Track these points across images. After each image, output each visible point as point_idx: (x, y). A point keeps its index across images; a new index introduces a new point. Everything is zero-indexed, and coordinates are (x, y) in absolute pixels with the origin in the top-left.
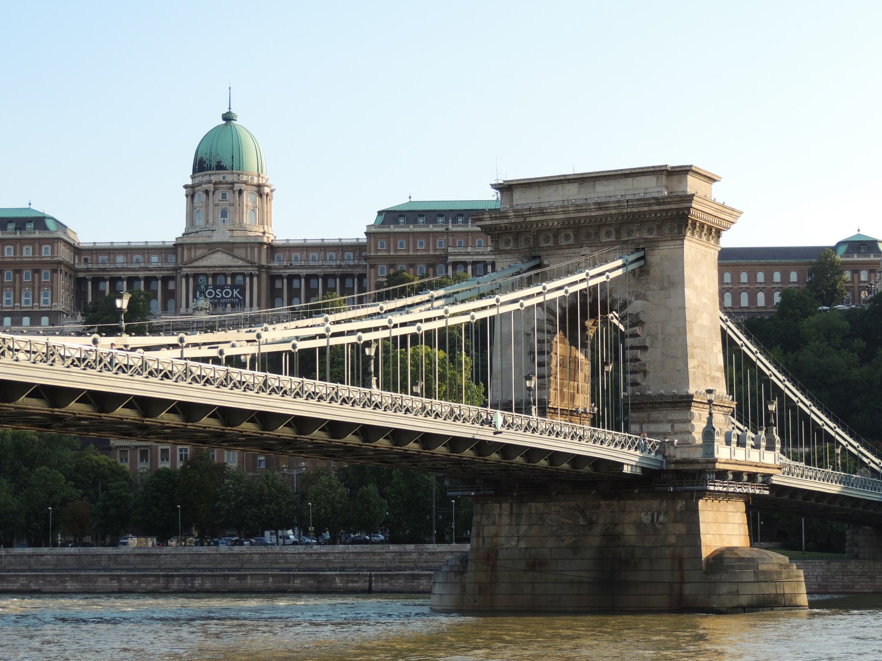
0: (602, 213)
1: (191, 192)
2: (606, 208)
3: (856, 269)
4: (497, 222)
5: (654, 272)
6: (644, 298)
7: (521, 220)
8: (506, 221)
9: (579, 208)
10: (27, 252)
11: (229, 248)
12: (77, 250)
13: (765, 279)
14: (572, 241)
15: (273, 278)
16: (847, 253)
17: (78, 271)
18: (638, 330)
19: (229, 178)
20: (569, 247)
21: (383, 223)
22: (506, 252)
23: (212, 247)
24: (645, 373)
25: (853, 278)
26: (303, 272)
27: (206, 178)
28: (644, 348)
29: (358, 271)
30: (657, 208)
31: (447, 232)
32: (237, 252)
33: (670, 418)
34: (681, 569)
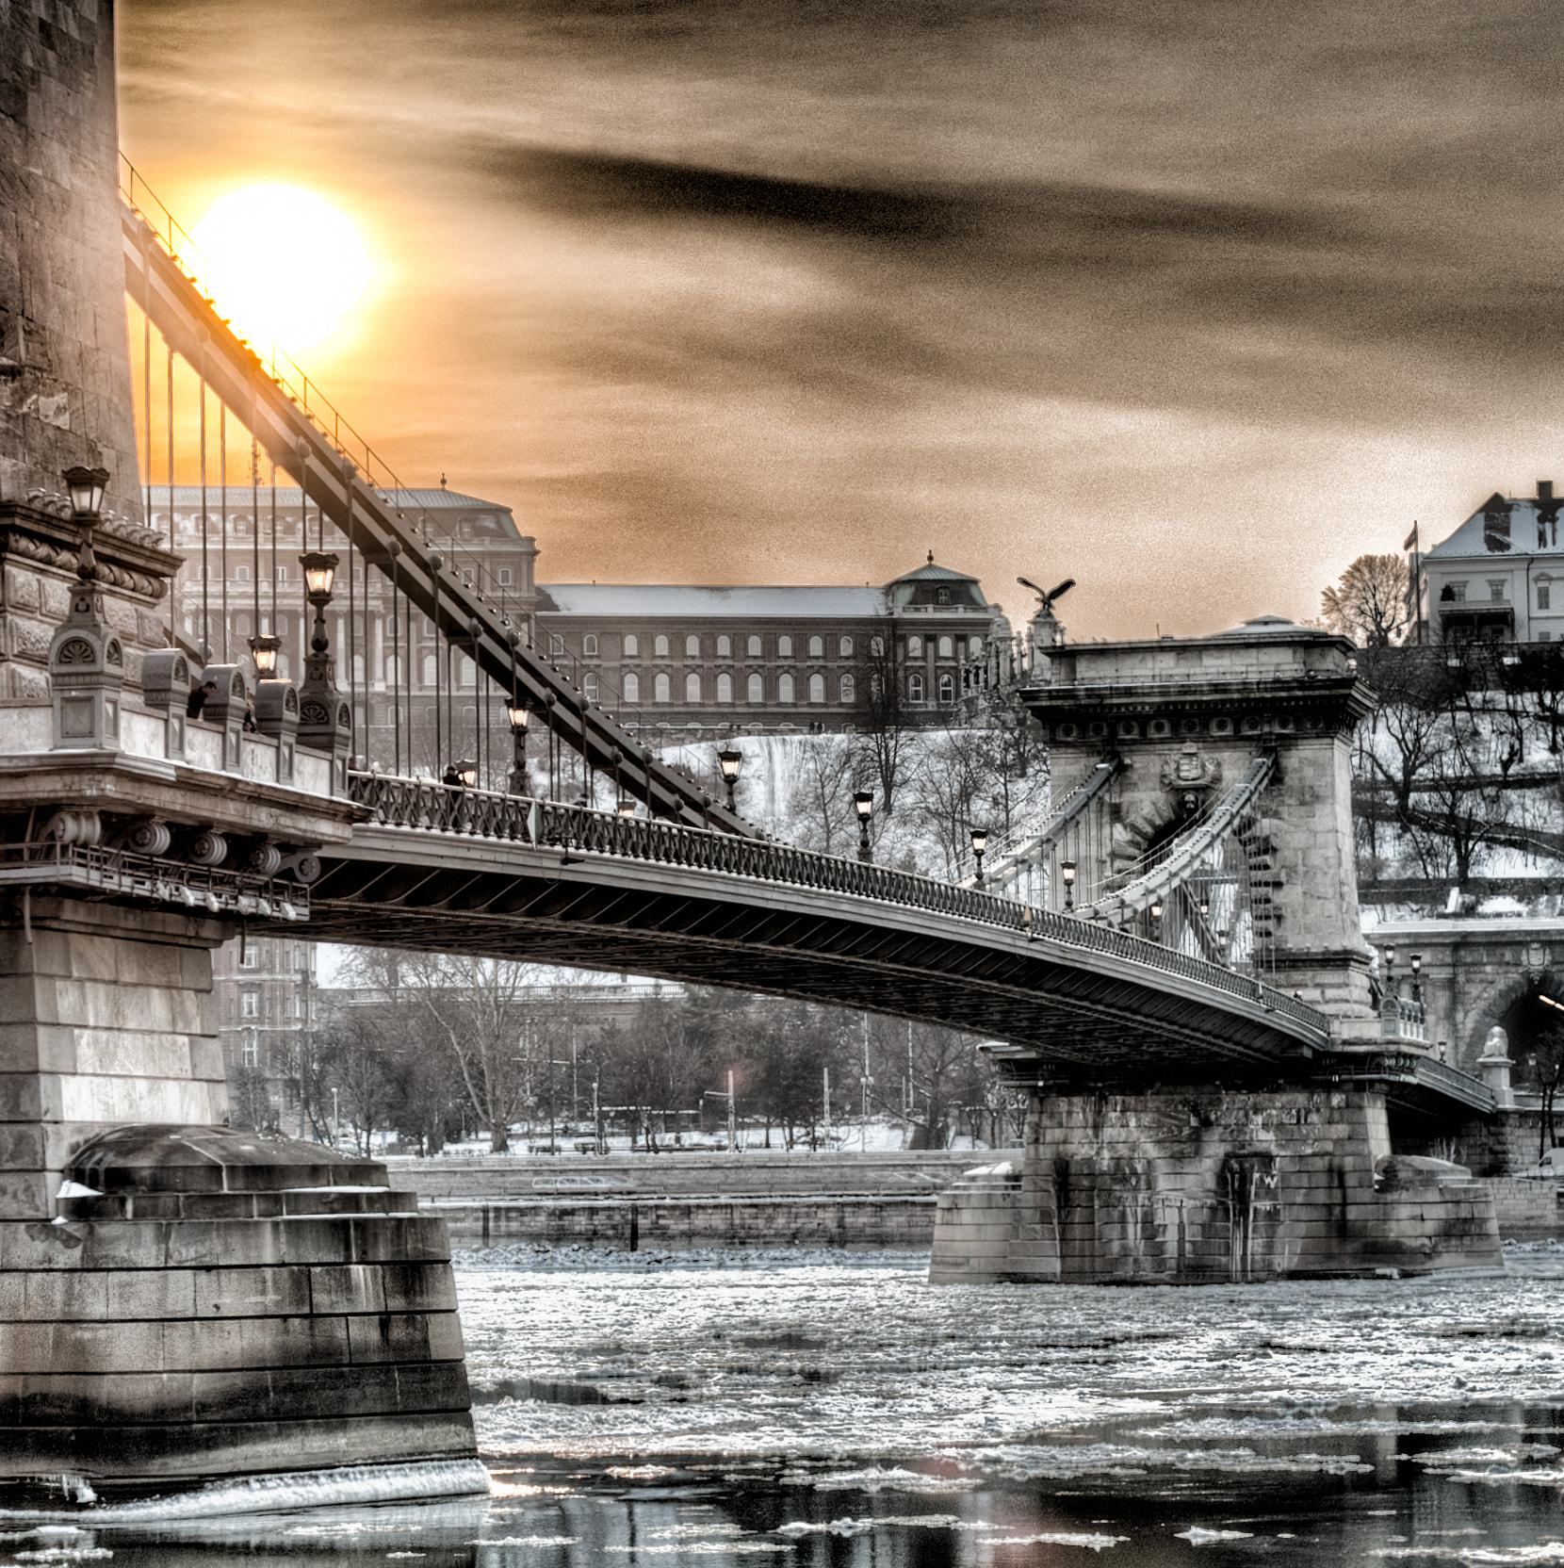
0: (1218, 697)
2: (1225, 691)
4: (1059, 703)
5: (1291, 779)
6: (1276, 815)
9: (1185, 690)
13: (794, 650)
14: (1166, 733)
18: (1268, 859)
20: (1162, 741)
22: (1067, 745)
24: (1279, 918)
25: (956, 650)
28: (1278, 885)
30: (1299, 693)
33: (1319, 980)
34: (1342, 1186)
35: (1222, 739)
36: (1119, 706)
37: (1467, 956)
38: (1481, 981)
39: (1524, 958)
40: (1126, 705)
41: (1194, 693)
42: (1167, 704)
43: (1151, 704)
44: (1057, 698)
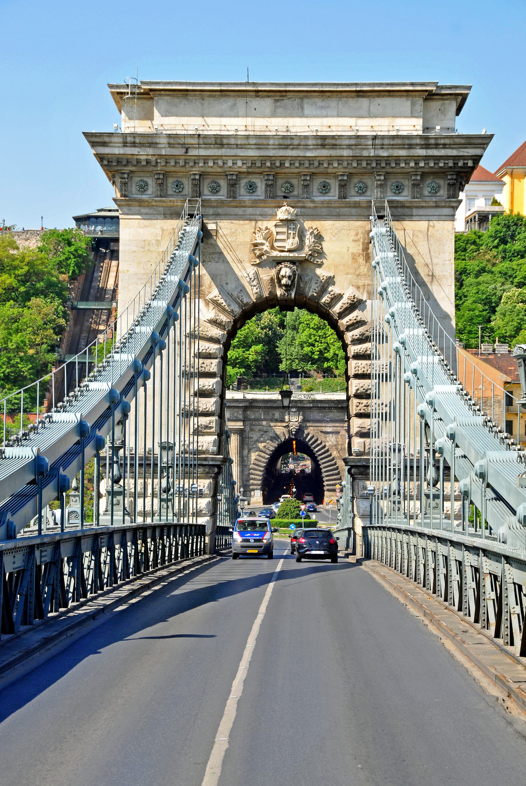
0: (325, 152)
2: (334, 146)
4: (135, 151)
7: (179, 151)
8: (150, 151)
20: (255, 204)
22: (141, 203)
30: (422, 152)
35: (328, 205)
36: (206, 159)
37: (251, 415)
38: (259, 430)
39: (287, 417)
40: (215, 159)
41: (297, 147)
42: (264, 159)
43: (244, 159)
44: (134, 144)
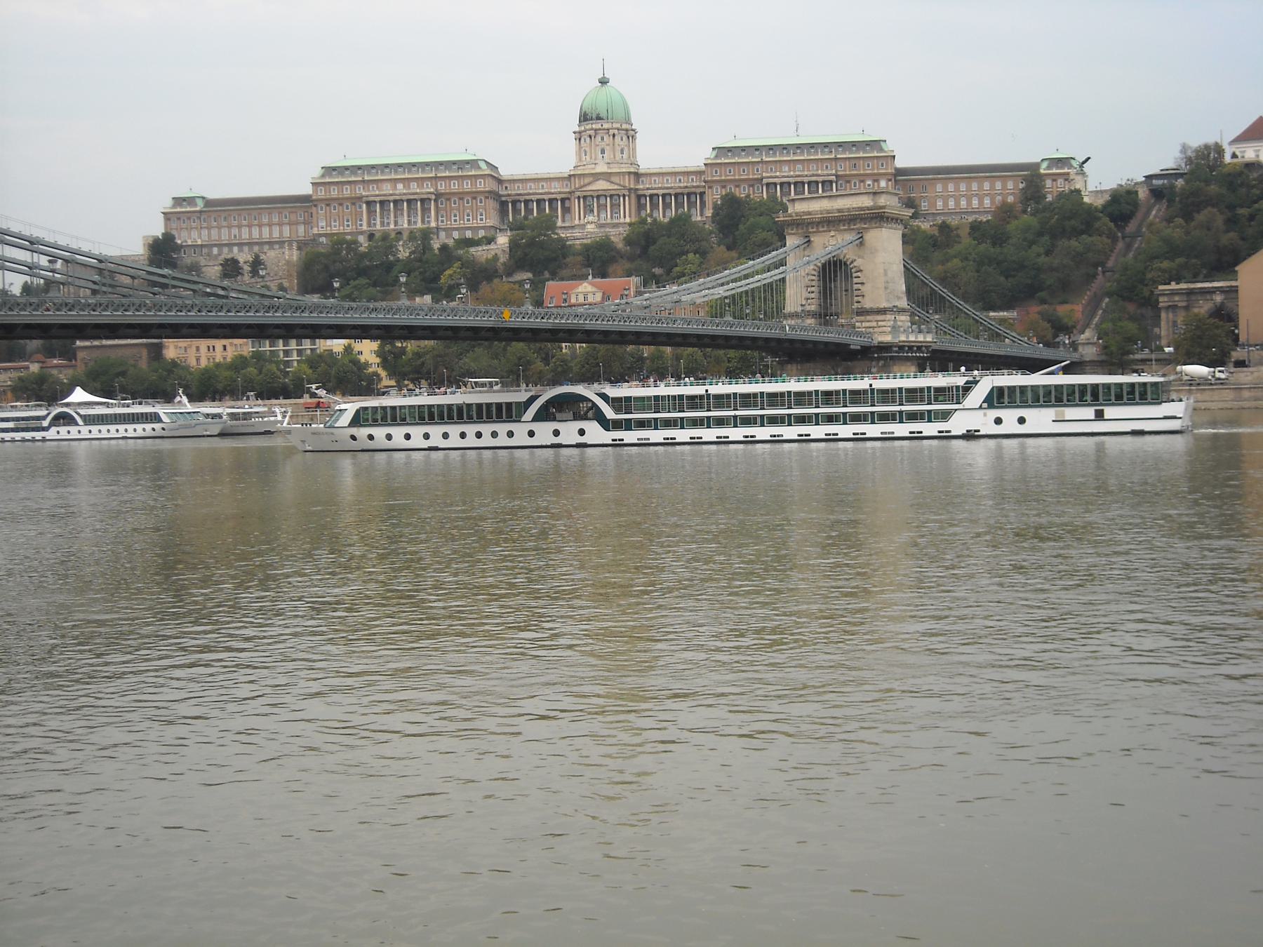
1: (579, 136)
3: (1054, 177)
10: (467, 186)
11: (607, 176)
12: (500, 181)
15: (639, 197)
16: (1049, 168)
17: (501, 196)
19: (606, 126)
21: (716, 157)
23: (597, 176)
26: (661, 192)
27: (589, 127)
29: (698, 191)
31: (762, 162)
32: (613, 179)
